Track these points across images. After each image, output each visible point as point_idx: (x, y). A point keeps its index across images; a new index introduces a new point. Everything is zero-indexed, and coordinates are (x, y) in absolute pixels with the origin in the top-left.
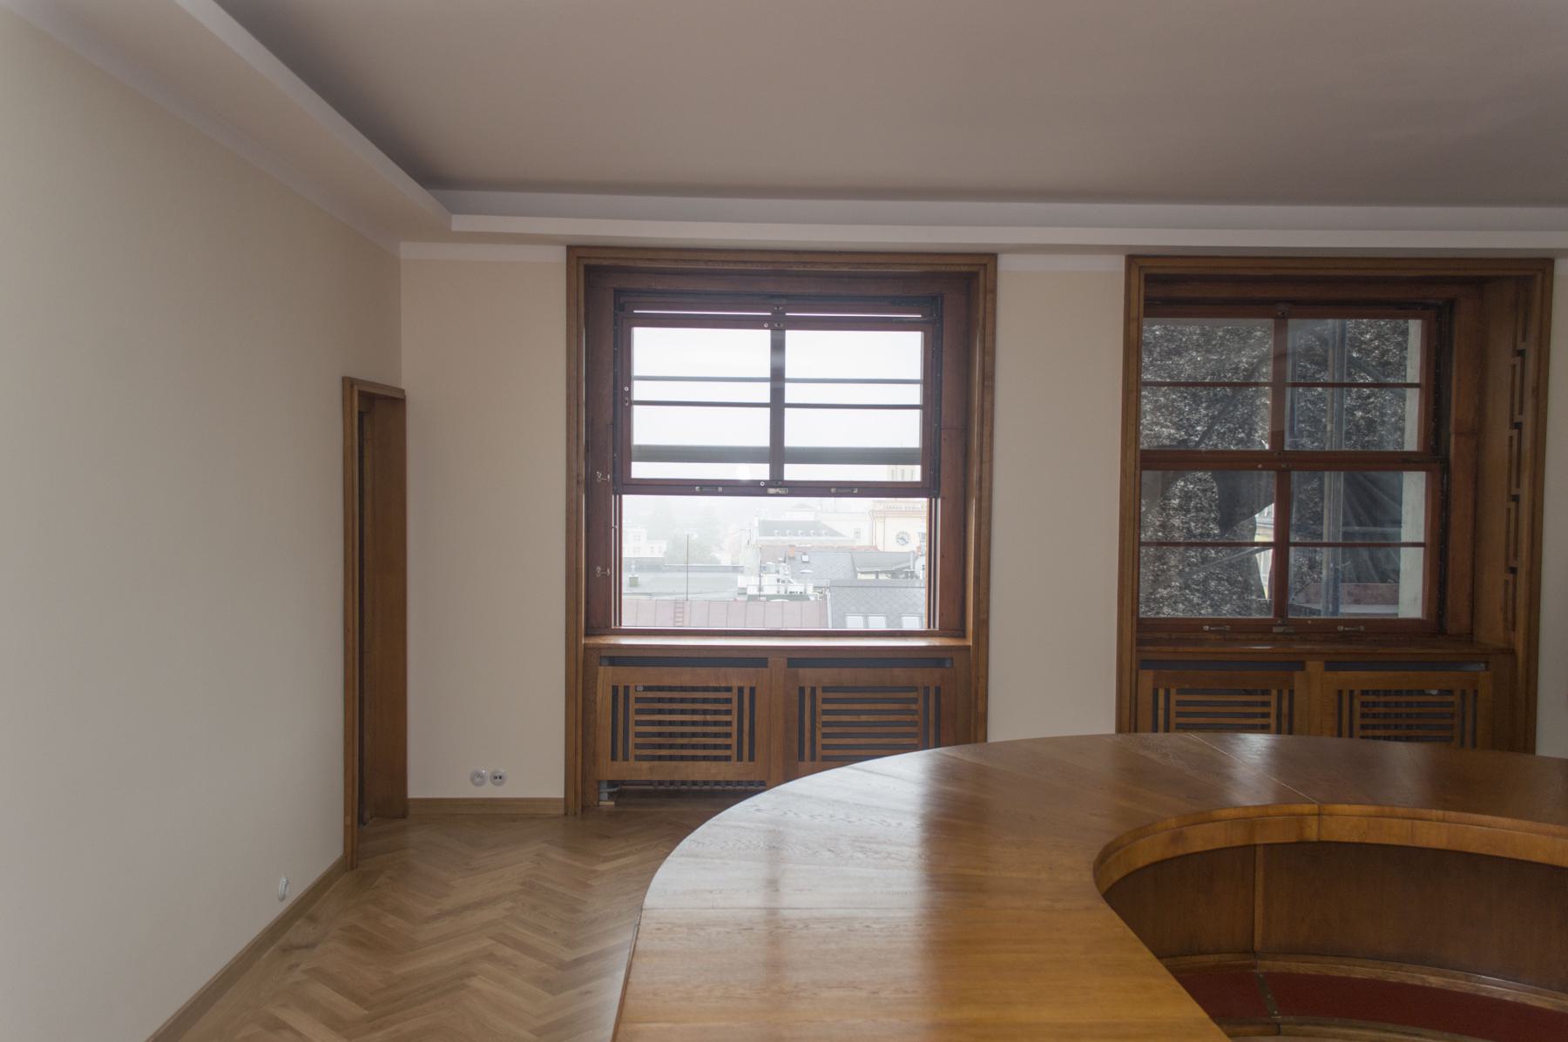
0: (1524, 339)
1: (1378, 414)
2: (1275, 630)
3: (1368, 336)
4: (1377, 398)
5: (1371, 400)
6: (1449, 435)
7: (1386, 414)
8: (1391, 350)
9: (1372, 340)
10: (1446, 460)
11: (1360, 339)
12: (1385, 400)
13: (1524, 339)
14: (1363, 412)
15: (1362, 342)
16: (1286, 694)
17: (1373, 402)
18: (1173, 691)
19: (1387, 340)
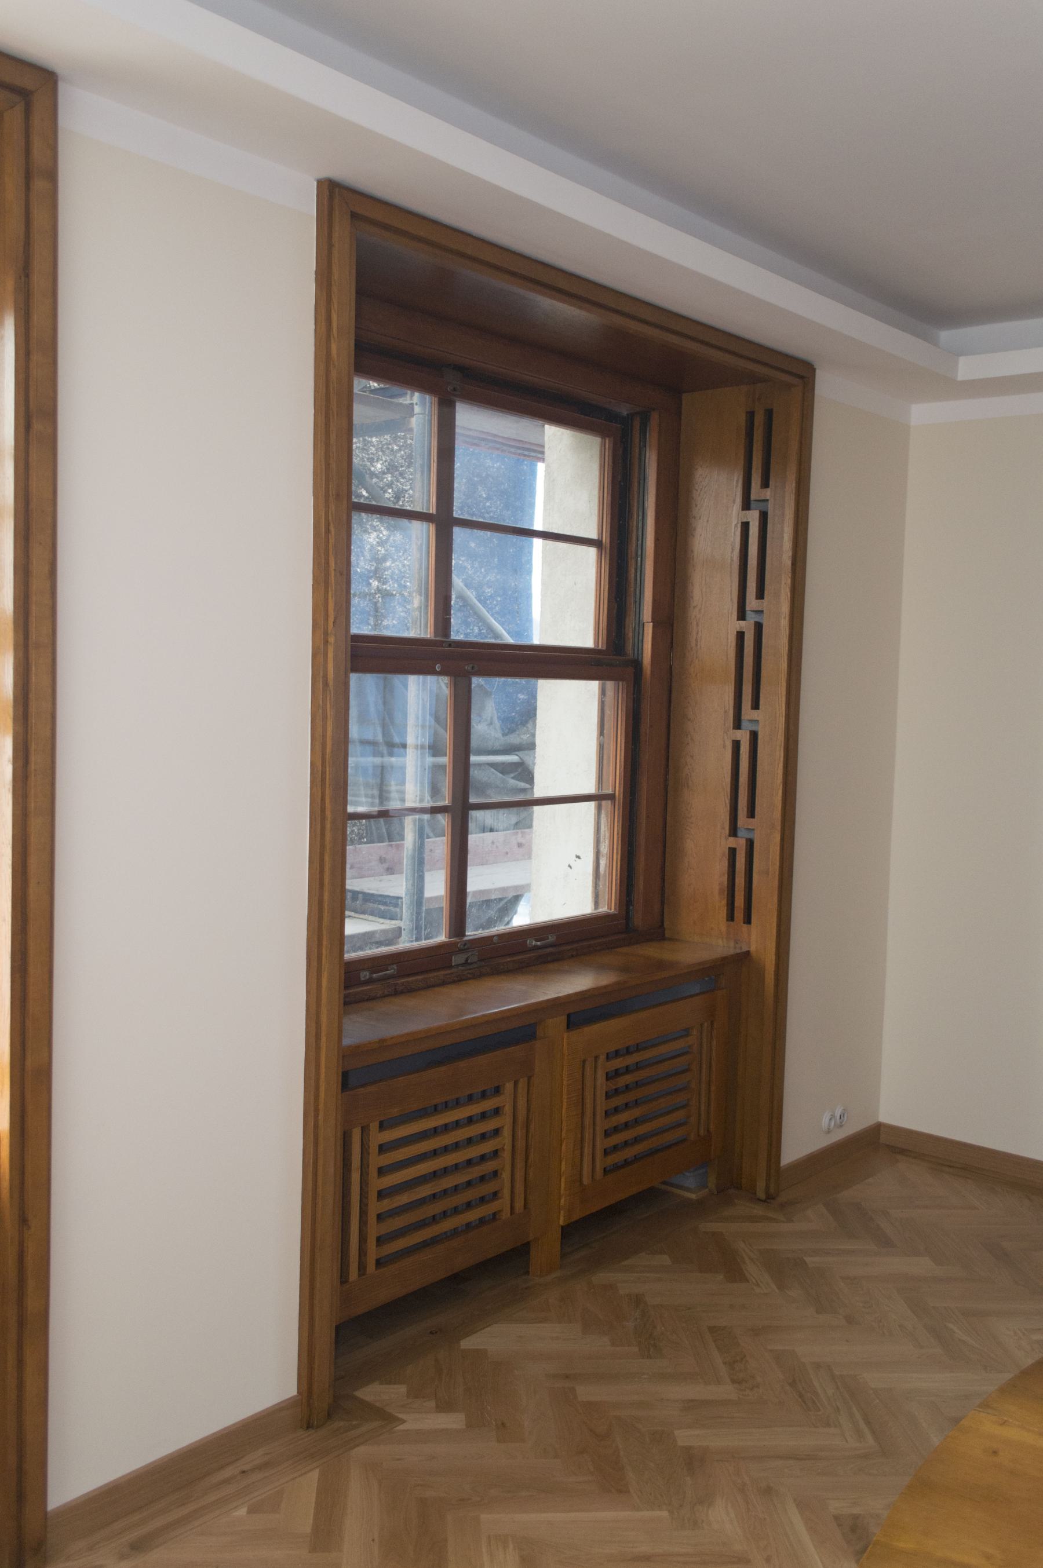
0: (765, 484)
1: (396, 585)
2: (457, 959)
3: (379, 466)
4: (394, 561)
5: (388, 564)
6: (641, 625)
7: (405, 587)
8: (406, 491)
9: (384, 473)
10: (637, 664)
11: (370, 470)
12: (404, 566)
13: (765, 484)
14: (379, 582)
15: (373, 475)
16: (523, 1083)
17: (390, 568)
18: (374, 1126)
19: (401, 474)
